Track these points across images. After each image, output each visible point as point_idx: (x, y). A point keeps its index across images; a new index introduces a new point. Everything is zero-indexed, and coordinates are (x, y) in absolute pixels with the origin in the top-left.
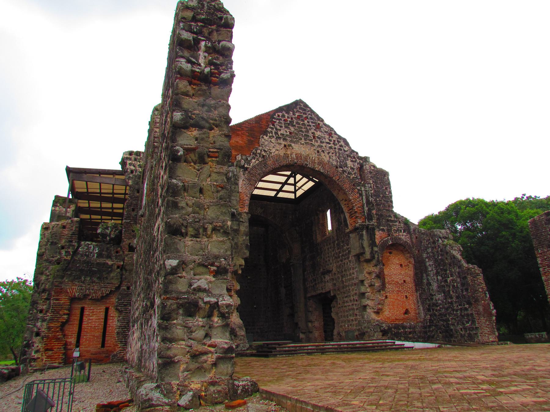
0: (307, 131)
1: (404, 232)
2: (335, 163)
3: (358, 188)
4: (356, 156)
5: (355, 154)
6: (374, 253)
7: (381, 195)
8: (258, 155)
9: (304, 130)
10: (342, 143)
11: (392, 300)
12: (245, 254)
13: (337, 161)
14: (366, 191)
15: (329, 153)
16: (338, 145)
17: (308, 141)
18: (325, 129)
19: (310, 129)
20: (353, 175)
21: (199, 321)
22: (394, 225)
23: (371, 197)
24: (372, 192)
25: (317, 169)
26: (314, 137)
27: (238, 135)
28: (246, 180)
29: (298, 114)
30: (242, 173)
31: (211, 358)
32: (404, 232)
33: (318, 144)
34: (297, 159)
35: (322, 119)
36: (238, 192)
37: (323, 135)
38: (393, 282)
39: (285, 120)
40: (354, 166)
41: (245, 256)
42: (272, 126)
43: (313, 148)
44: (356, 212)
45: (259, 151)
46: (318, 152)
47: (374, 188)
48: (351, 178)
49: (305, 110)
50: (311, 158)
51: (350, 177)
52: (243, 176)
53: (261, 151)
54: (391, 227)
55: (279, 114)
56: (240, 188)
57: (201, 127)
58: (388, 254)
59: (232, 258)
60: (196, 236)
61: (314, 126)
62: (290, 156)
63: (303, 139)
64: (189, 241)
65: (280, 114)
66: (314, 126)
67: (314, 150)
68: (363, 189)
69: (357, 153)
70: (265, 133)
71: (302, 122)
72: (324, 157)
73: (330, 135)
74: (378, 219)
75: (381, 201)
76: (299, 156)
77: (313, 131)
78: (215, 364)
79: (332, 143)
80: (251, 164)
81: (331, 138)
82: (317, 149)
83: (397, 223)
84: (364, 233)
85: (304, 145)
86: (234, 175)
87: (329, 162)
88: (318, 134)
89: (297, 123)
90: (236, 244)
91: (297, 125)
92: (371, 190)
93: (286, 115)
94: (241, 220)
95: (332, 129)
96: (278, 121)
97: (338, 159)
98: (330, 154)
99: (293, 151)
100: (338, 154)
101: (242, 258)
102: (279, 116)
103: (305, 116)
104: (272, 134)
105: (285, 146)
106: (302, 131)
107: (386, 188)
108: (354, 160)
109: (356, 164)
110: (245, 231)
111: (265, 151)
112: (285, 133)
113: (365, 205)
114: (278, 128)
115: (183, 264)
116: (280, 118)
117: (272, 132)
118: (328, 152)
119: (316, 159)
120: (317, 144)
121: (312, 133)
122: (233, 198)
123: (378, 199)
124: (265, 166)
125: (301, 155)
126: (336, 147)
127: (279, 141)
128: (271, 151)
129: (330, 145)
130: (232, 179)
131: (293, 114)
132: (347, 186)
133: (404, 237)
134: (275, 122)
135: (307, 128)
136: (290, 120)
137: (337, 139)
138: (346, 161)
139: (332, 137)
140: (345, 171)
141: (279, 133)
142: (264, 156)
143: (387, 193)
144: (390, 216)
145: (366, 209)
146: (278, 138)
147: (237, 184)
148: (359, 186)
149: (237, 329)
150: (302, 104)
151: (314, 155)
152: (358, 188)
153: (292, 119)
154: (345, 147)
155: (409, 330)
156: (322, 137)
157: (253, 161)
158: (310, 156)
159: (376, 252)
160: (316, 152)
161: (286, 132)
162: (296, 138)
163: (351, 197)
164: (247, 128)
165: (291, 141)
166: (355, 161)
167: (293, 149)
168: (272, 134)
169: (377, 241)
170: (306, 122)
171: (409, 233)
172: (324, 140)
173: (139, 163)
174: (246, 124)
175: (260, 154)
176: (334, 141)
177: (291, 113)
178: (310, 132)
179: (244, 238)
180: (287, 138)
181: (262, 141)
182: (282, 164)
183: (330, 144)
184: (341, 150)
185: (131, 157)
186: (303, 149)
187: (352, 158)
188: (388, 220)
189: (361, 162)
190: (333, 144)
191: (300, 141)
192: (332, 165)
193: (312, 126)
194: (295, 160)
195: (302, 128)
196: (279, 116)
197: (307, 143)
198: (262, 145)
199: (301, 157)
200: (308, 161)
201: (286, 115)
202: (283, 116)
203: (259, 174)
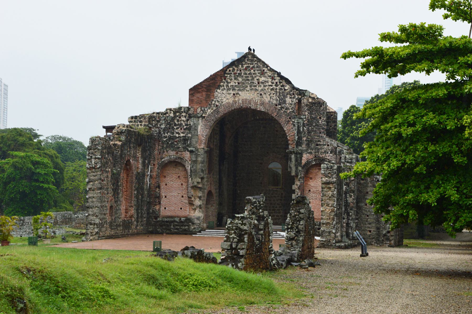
0: (253, 79)
1: (331, 153)
2: (275, 102)
3: (293, 120)
4: (295, 93)
5: (295, 91)
6: (298, 171)
7: (314, 124)
8: (213, 106)
9: (249, 78)
10: (284, 83)
11: (314, 205)
12: (200, 175)
13: (277, 100)
14: (298, 123)
15: (271, 94)
16: (280, 86)
17: (253, 87)
18: (269, 74)
19: (255, 77)
20: (290, 110)
21: (92, 226)
22: (322, 148)
23: (304, 125)
24: (306, 122)
25: (258, 109)
26: (259, 83)
27: (199, 92)
28: (203, 126)
29: (246, 66)
30: (200, 121)
31: (94, 233)
32: (331, 153)
33: (261, 88)
34: (243, 103)
35: (267, 65)
36: (197, 135)
37: (267, 80)
38: (317, 192)
39: (235, 74)
40: (292, 102)
41: (201, 177)
42: (224, 81)
43: (256, 93)
44: (289, 140)
45: (214, 102)
46: (261, 95)
47: (308, 119)
48: (288, 112)
49: (252, 61)
50: (254, 101)
51: (287, 112)
52: (201, 123)
53: (215, 102)
54: (319, 149)
55: (230, 69)
56: (199, 132)
57: (93, 182)
58: (317, 170)
59: (192, 179)
60: (92, 208)
61: (259, 73)
62: (237, 102)
63: (249, 86)
64: (91, 209)
65: (231, 69)
66: (259, 73)
67: (258, 94)
68: (296, 121)
69: (297, 89)
70: (219, 87)
71: (249, 72)
72: (265, 98)
73: (273, 78)
74: (308, 145)
75: (313, 129)
76: (244, 101)
77: (257, 78)
78: (95, 234)
79: (274, 85)
80: (208, 113)
81: (273, 81)
82: (260, 93)
83: (326, 147)
84: (293, 156)
85: (249, 91)
86: (194, 124)
87: (269, 101)
88: (262, 79)
89: (246, 74)
90: (194, 169)
91: (244, 76)
92: (305, 121)
93: (236, 69)
94: (199, 153)
95: (276, 72)
96: (229, 76)
97: (278, 98)
98: (272, 95)
99: (240, 98)
100: (278, 94)
101: (199, 178)
102: (230, 71)
103: (251, 66)
104: (224, 87)
105: (234, 94)
106: (248, 80)
107: (320, 118)
108: (293, 96)
109: (295, 100)
110: (201, 160)
111: (218, 101)
112: (234, 84)
113: (296, 135)
114: (229, 81)
115: (89, 215)
116: (231, 72)
117: (223, 85)
118: (269, 93)
119: (259, 101)
120: (260, 88)
121: (257, 80)
122: (193, 140)
123: (310, 128)
124: (217, 113)
125: (246, 99)
126: (278, 88)
127: (229, 92)
128: (223, 101)
129: (272, 87)
130: (193, 127)
131: (242, 67)
132: (282, 120)
133: (330, 157)
134: (227, 76)
135: (252, 77)
136: (239, 72)
137: (279, 80)
138: (285, 98)
139: (275, 80)
140: (283, 108)
141: (229, 85)
142: (217, 106)
143: (320, 122)
144: (319, 141)
145: (297, 137)
146: (229, 89)
147: (196, 130)
148: (295, 118)
149: (195, 220)
150: (250, 56)
151: (257, 99)
152: (293, 120)
153: (240, 71)
154: (286, 86)
155: (318, 227)
156: (265, 81)
157: (209, 110)
158: (254, 99)
159: (300, 170)
160: (259, 95)
161: (235, 83)
162: (243, 87)
163: (285, 129)
164: (206, 85)
165: (239, 90)
166: (294, 98)
167: (240, 95)
168: (224, 87)
169: (304, 161)
170: (252, 71)
171: (335, 154)
172: (267, 84)
173: (137, 124)
174: (205, 82)
175: (214, 104)
176: (277, 83)
177: (240, 66)
178: (255, 79)
179: (201, 165)
180: (236, 88)
181: (216, 94)
182: (231, 109)
183: (272, 86)
184: (282, 89)
185: (132, 120)
186: (248, 95)
187: (291, 95)
188: (317, 145)
189: (300, 97)
190: (275, 85)
191: (247, 89)
192: (272, 103)
193: (257, 74)
194: (241, 105)
195: (248, 77)
196: (230, 71)
197: (252, 89)
198: (216, 97)
199: (246, 101)
200: (252, 103)
201: (236, 69)
202: (234, 69)
203: (213, 120)
